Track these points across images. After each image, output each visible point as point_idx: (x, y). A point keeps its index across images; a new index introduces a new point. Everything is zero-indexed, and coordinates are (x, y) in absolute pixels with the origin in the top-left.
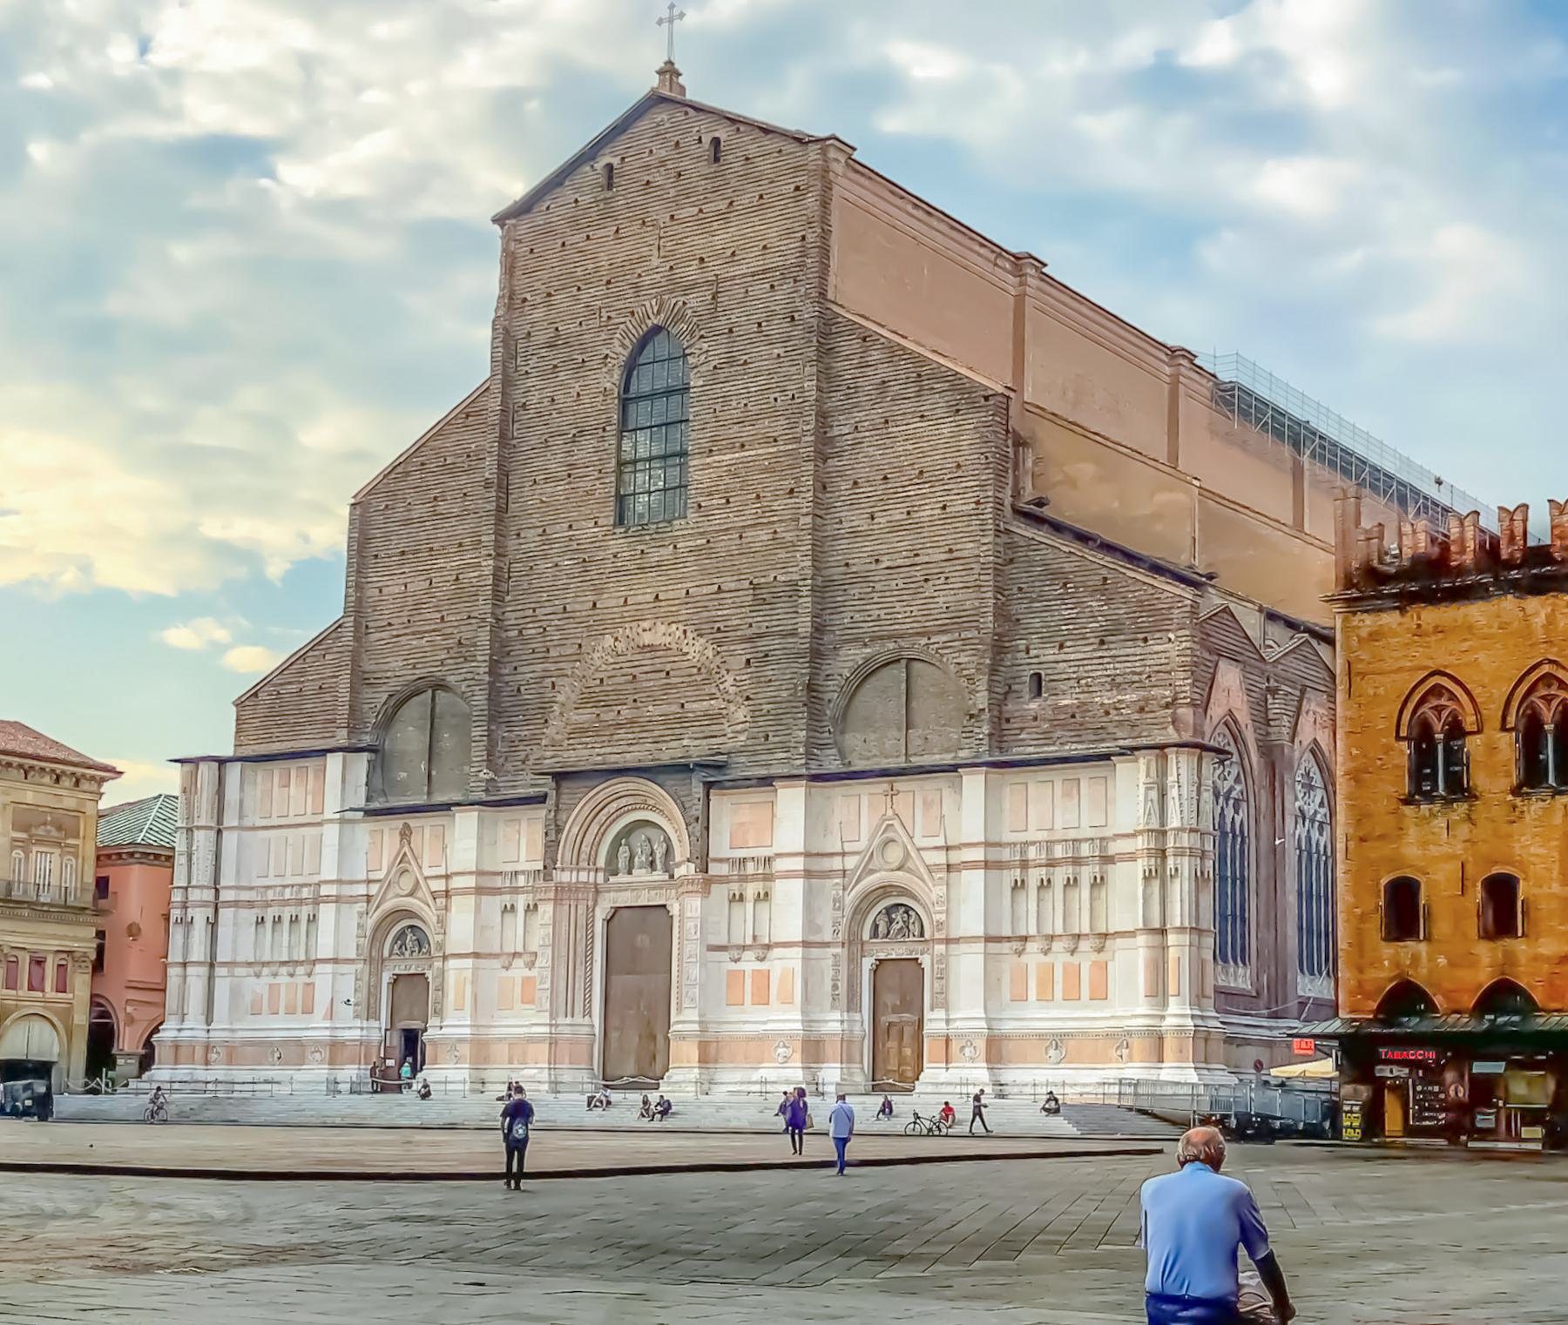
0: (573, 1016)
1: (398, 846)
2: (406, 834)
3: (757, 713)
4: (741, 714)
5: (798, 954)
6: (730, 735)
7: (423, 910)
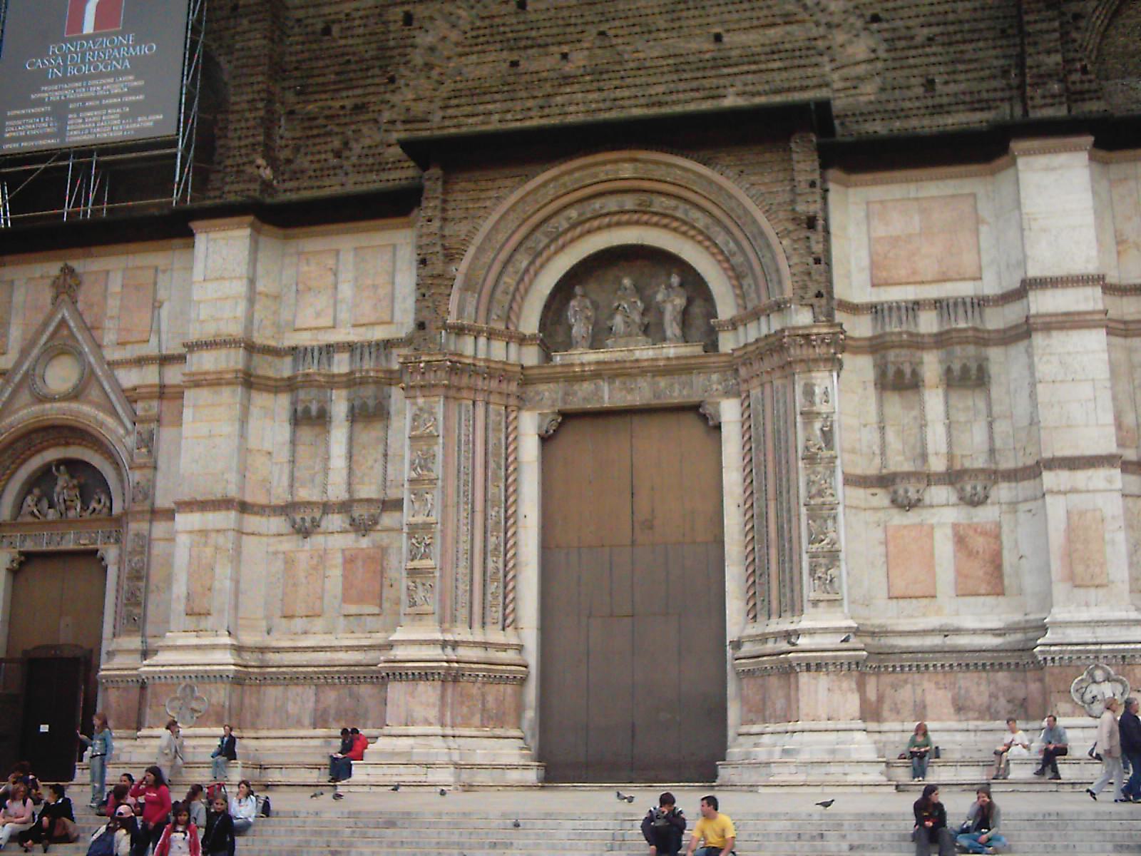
1: (49, 307)
2: (67, 286)
3: (902, 44)
4: (860, 49)
5: (1110, 481)
6: (836, 86)
7: (102, 424)
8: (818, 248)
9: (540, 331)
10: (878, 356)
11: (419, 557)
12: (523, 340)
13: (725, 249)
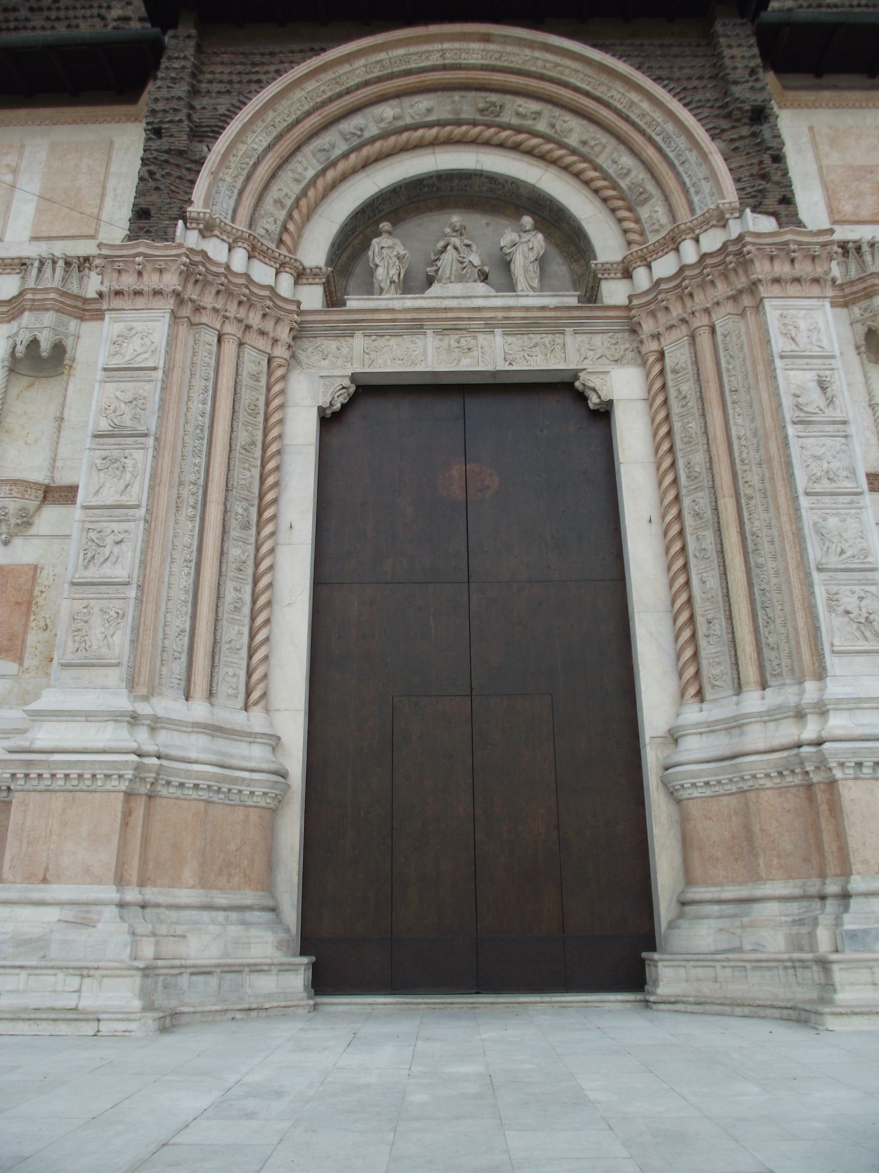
0: (211, 694)
8: (774, 143)
9: (327, 265)
10: (856, 310)
11: (99, 559)
12: (301, 275)
13: (611, 171)
